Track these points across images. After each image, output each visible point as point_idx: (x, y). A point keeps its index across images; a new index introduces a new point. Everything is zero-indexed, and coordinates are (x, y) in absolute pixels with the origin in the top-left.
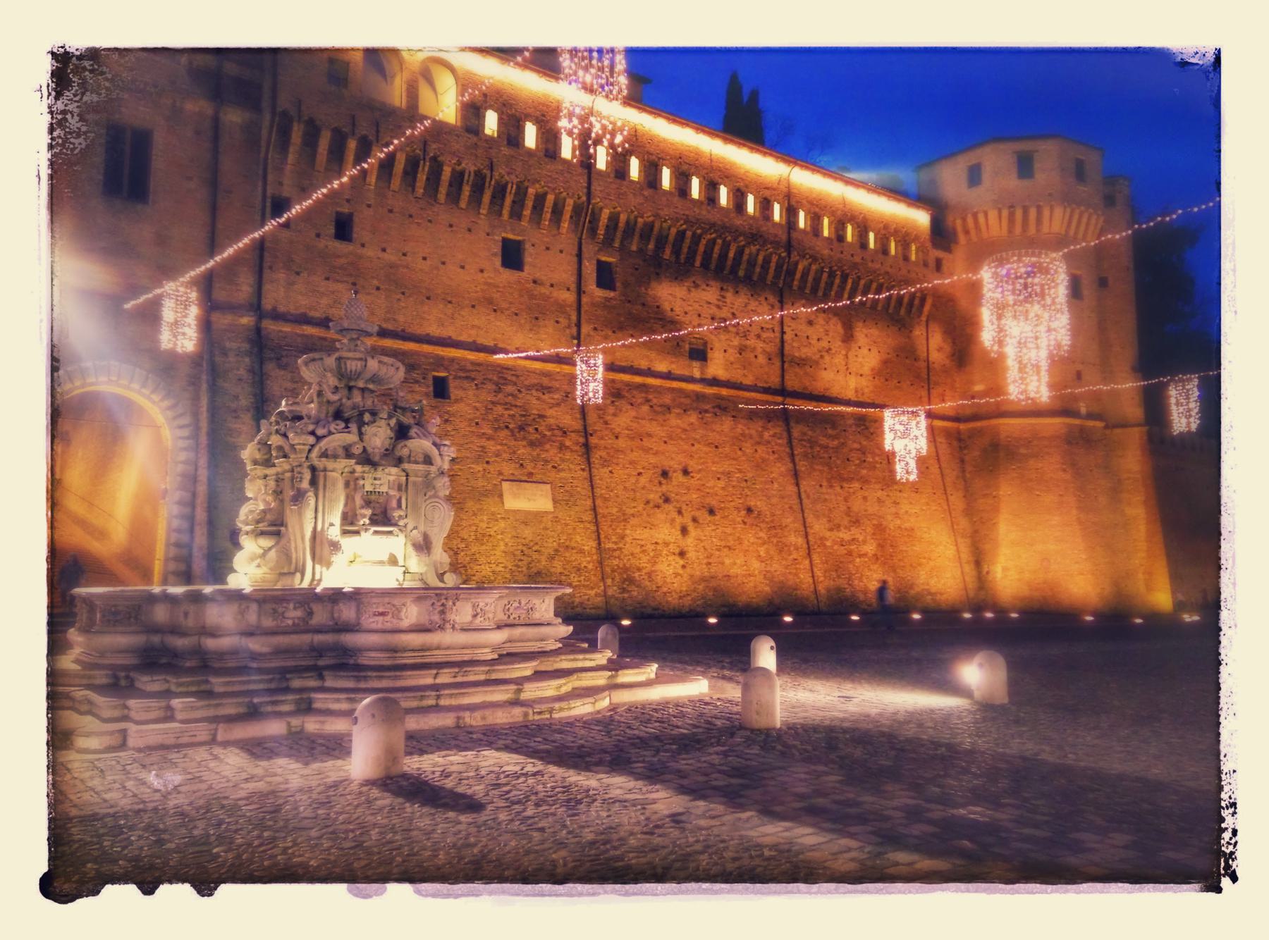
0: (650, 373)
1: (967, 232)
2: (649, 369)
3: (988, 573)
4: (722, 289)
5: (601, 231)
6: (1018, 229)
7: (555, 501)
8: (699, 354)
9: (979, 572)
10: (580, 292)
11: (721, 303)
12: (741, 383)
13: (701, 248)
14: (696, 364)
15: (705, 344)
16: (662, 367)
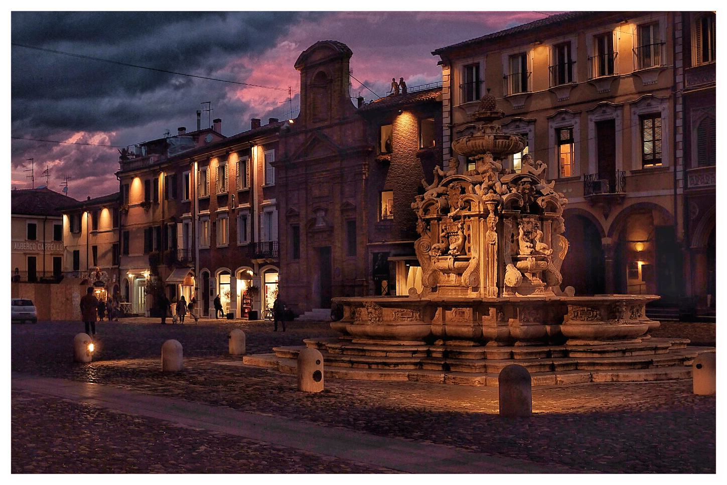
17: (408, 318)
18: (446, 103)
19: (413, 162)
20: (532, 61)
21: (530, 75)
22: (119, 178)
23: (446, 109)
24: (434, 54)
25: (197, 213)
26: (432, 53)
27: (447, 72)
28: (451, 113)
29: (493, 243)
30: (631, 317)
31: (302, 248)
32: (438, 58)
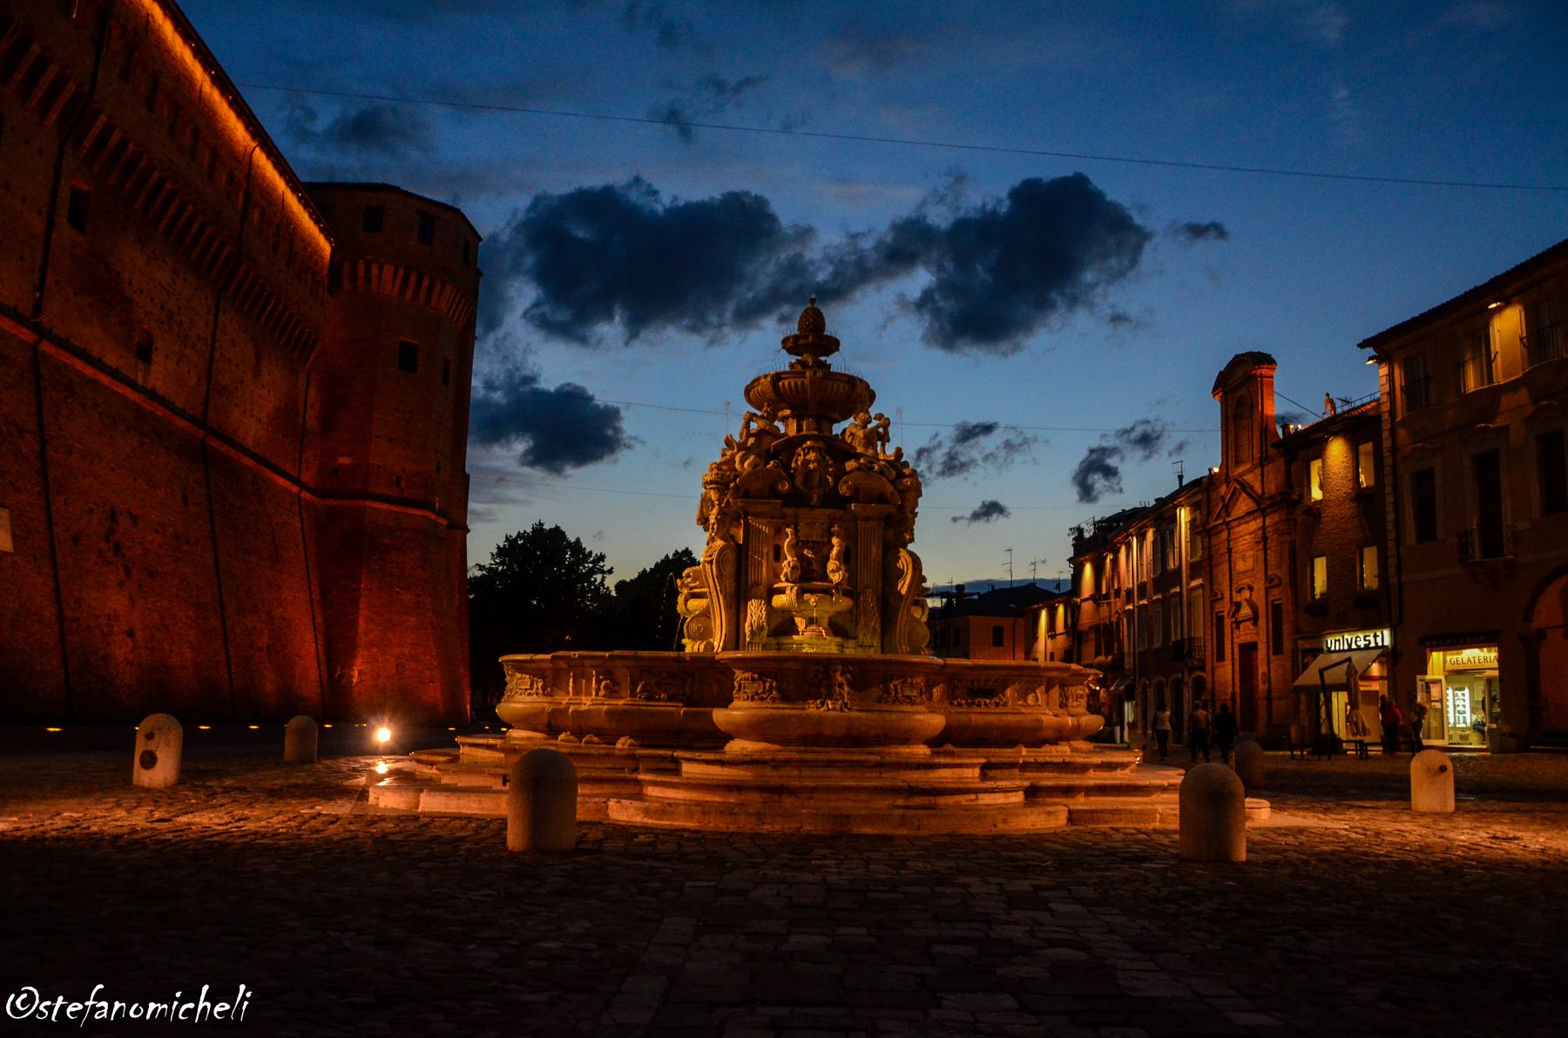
0: (98, 364)
1: (354, 278)
2: (100, 359)
3: (341, 676)
4: (175, 272)
5: (87, 144)
6: (409, 295)
7: (15, 537)
8: (144, 353)
9: (331, 675)
10: (50, 225)
11: (171, 290)
12: (173, 403)
13: (171, 211)
14: (141, 366)
15: (150, 340)
16: (111, 360)
17: (526, 690)
18: (1386, 417)
19: (1348, 509)
20: (1497, 334)
21: (1495, 357)
22: (1071, 565)
23: (1386, 426)
24: (1362, 345)
25: (1136, 604)
26: (1359, 345)
27: (1384, 370)
28: (1393, 432)
29: (709, 559)
30: (881, 698)
31: (1228, 647)
32: (1370, 351)
